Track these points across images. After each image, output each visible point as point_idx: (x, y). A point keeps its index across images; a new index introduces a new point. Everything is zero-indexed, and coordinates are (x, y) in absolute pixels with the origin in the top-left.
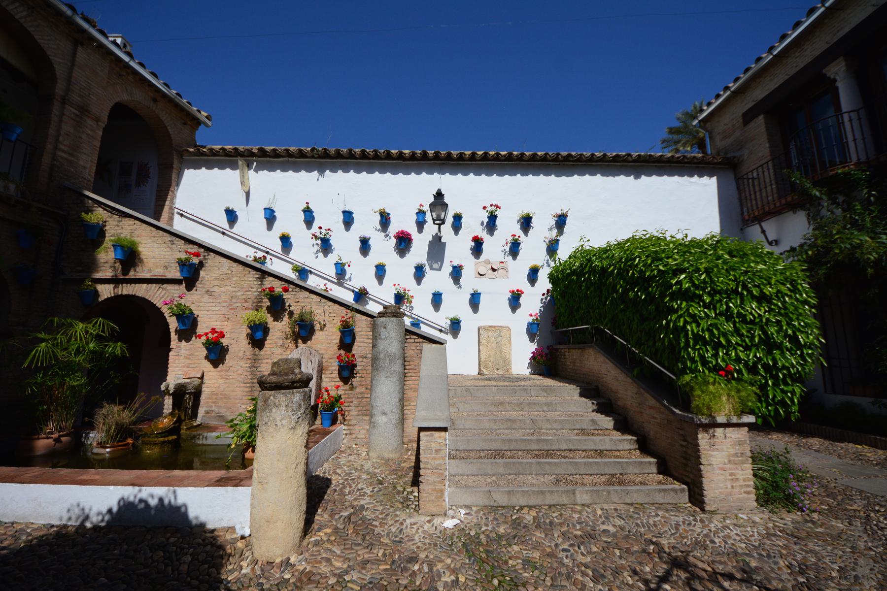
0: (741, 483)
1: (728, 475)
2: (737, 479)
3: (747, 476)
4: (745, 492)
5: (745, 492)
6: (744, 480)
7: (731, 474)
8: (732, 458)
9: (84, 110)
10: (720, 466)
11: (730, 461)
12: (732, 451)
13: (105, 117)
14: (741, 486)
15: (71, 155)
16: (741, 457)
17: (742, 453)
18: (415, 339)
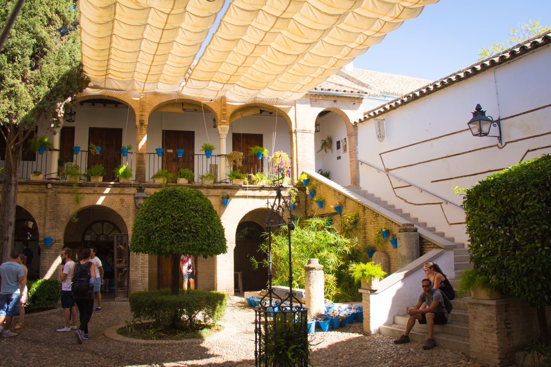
0: (490, 345)
1: (483, 338)
2: (488, 342)
3: (494, 341)
4: (492, 352)
5: (492, 352)
6: (492, 343)
7: (485, 338)
8: (486, 328)
9: (304, 131)
10: (479, 331)
11: (484, 329)
12: (486, 323)
13: (313, 129)
14: (490, 347)
15: (303, 156)
16: (491, 327)
17: (491, 326)
18: (430, 245)
